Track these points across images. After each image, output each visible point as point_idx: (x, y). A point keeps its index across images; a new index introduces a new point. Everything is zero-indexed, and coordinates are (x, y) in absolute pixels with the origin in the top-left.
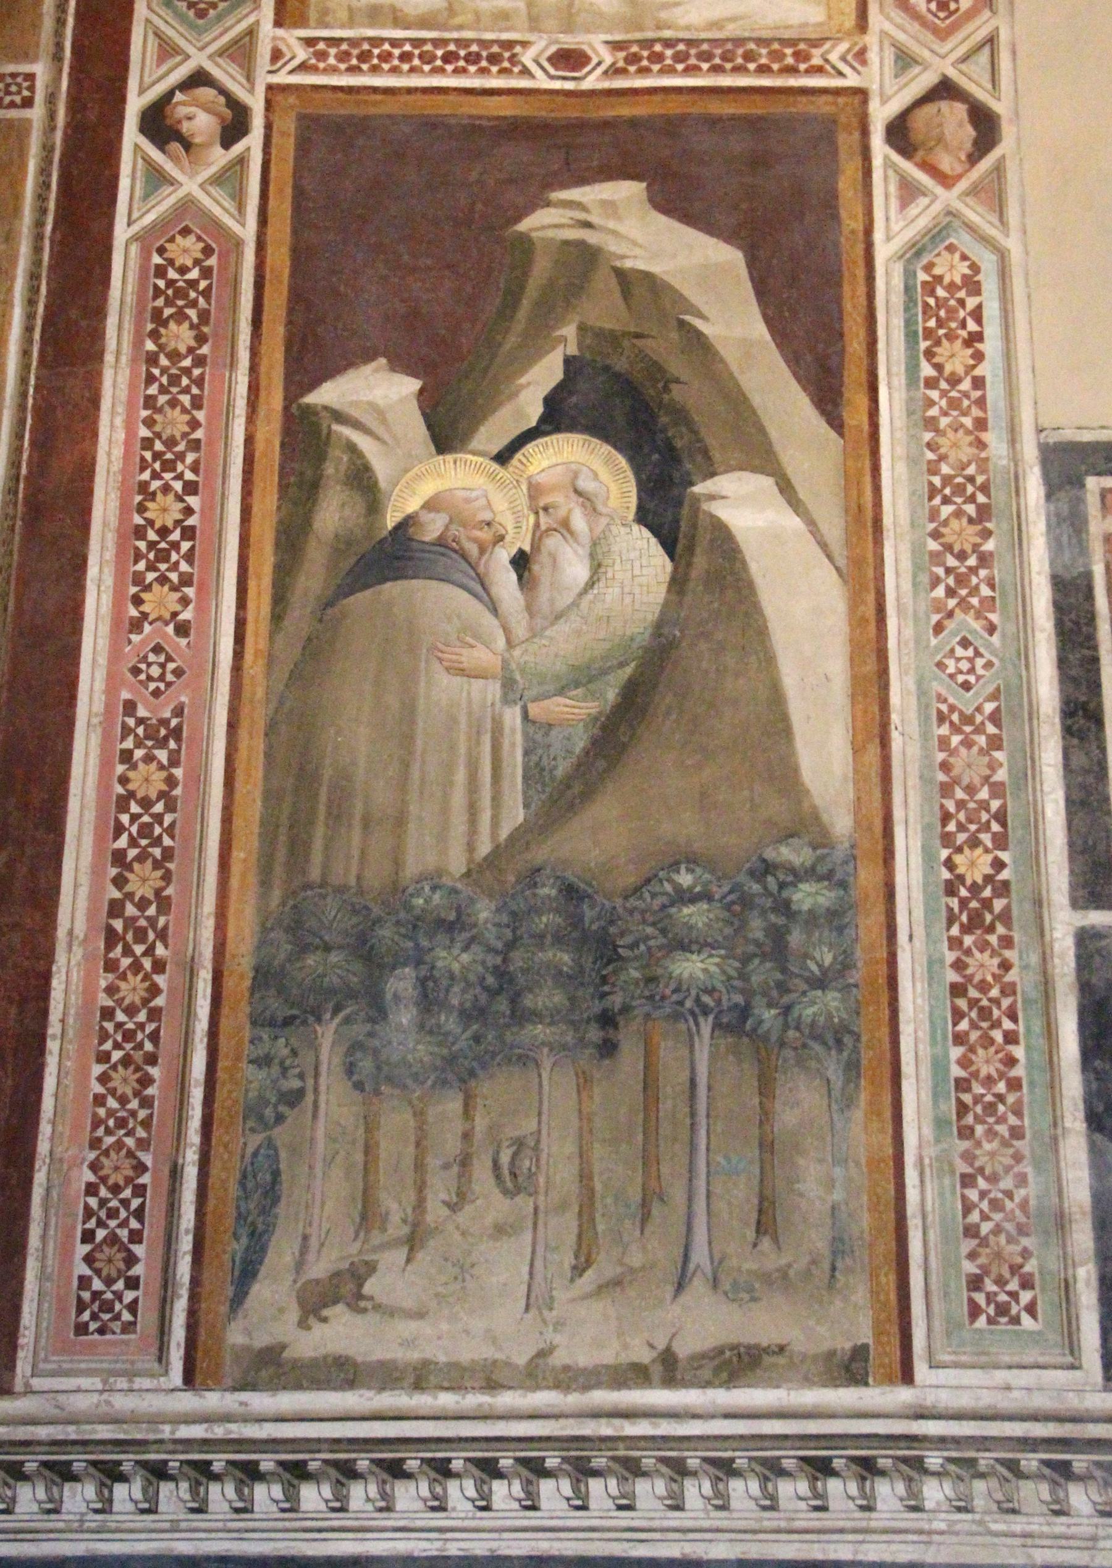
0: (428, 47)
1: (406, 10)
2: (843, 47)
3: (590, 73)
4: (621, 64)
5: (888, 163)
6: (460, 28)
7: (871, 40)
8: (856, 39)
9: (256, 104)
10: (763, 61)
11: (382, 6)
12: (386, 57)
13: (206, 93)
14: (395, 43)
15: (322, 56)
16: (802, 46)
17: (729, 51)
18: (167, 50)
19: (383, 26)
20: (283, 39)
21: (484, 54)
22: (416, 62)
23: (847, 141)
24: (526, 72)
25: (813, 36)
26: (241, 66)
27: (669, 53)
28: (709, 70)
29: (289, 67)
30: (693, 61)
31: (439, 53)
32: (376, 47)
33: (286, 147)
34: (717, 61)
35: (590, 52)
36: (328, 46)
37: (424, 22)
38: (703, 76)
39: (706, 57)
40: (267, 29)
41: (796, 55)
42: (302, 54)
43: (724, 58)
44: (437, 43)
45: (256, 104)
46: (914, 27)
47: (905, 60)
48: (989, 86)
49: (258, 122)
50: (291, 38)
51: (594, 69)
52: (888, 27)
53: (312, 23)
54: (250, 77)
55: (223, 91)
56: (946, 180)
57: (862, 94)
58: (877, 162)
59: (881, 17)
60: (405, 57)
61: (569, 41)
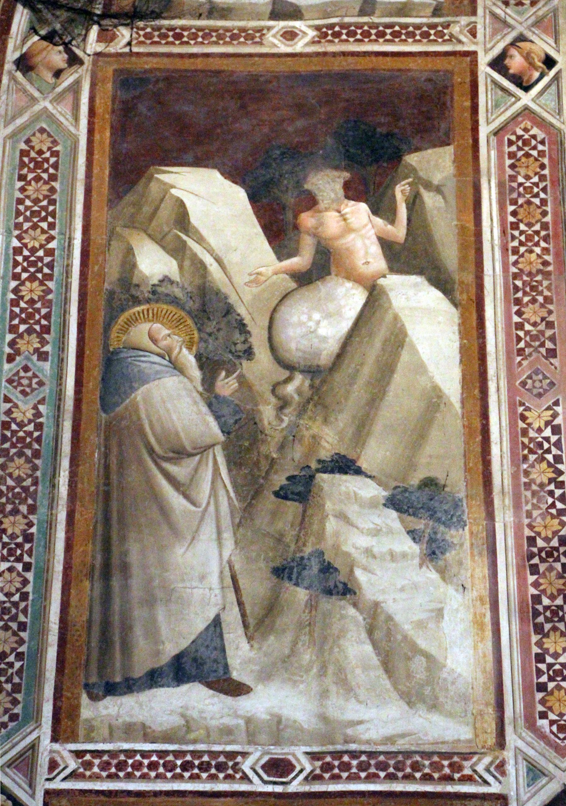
0: (170, 758)
1: (154, 727)
2: (487, 760)
3: (294, 778)
4: (318, 771)
6: (194, 742)
7: (508, 755)
8: (497, 753)
10: (427, 770)
11: (135, 724)
12: (138, 766)
14: (145, 754)
15: (88, 765)
16: (456, 759)
17: (399, 762)
19: (134, 741)
20: (58, 752)
21: (213, 763)
22: (161, 770)
24: (245, 778)
25: (464, 751)
26: (26, 776)
27: (354, 763)
28: (385, 777)
29: (62, 775)
30: (373, 770)
31: (179, 762)
32: (130, 758)
34: (391, 770)
36: (93, 757)
37: (167, 738)
38: (380, 783)
39: (383, 766)
41: (451, 765)
42: (73, 764)
43: (397, 768)
44: (178, 754)
46: (541, 745)
51: (297, 775)
52: (520, 744)
53: (81, 738)
54: (32, 785)
59: (515, 737)
60: (153, 766)
61: (278, 752)
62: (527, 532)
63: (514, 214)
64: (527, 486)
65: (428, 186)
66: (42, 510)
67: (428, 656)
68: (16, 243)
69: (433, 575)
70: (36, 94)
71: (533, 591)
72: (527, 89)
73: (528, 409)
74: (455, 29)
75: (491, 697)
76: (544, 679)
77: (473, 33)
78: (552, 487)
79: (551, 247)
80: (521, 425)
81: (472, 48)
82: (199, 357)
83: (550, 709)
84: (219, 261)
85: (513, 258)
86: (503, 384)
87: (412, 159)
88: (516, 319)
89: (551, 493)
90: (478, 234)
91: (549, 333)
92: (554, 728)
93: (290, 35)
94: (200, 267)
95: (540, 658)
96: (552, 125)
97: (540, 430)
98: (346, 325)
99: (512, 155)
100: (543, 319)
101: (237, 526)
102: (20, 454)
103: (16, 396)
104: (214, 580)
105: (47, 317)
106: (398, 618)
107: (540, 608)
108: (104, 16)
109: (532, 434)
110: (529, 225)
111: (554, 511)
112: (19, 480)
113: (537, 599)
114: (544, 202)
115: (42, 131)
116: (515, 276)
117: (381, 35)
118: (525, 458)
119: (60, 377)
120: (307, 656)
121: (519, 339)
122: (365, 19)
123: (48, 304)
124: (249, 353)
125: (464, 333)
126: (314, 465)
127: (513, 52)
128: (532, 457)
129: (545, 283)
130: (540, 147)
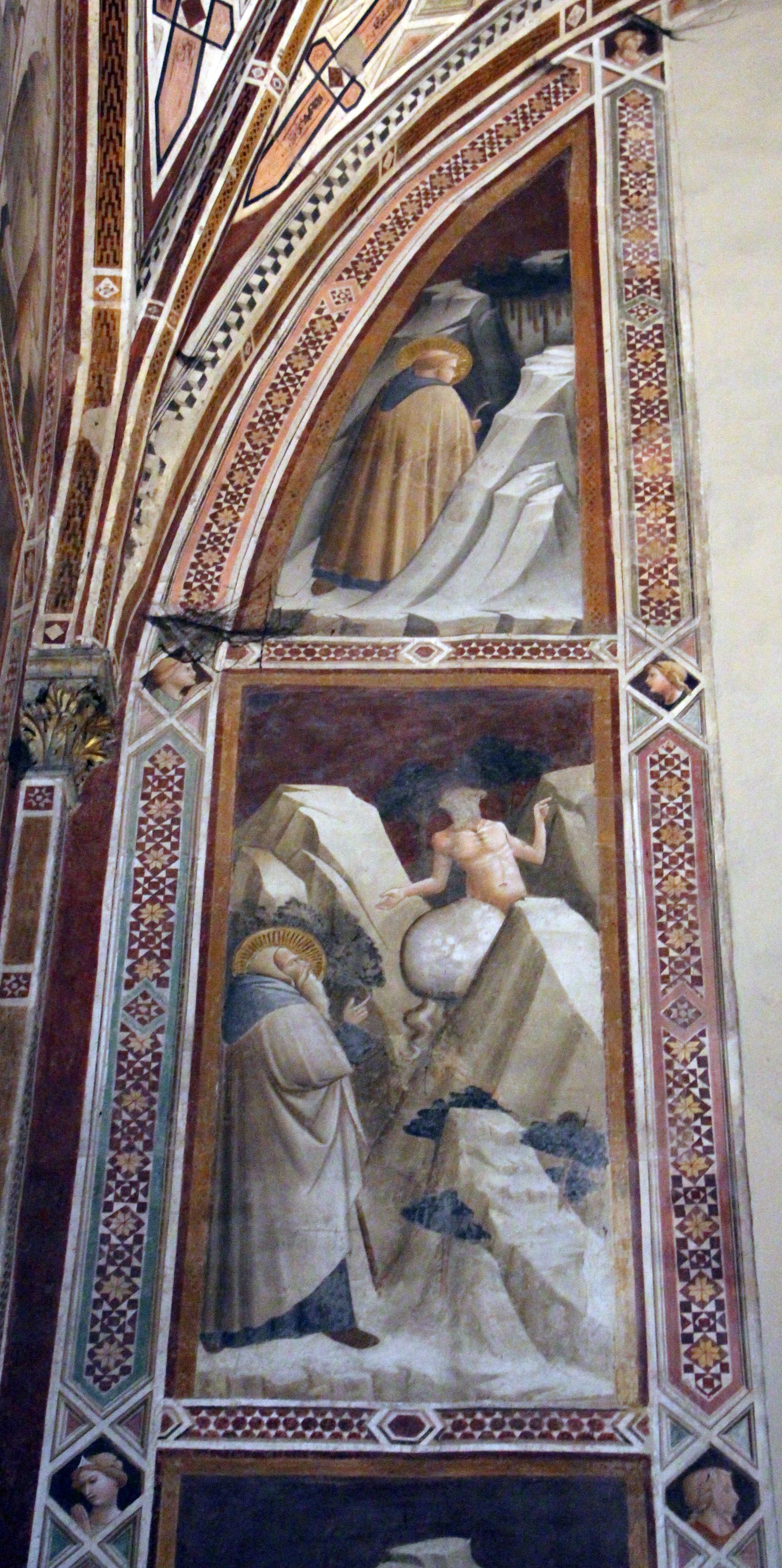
0: (291, 1415)
1: (274, 1381)
2: (629, 1417)
3: (424, 1437)
4: (449, 1430)
5: (668, 1524)
6: (317, 1397)
7: (651, 1412)
8: (640, 1410)
9: (148, 1467)
10: (565, 1429)
11: (254, 1378)
12: (256, 1424)
13: (107, 1458)
14: (265, 1411)
15: (204, 1423)
16: (596, 1416)
18: (76, 1420)
19: (254, 1396)
20: (171, 1408)
21: (337, 1421)
22: (281, 1428)
23: (634, 1502)
24: (371, 1437)
25: (604, 1407)
26: (137, 1433)
27: (488, 1420)
29: (176, 1434)
30: (507, 1428)
31: (300, 1420)
32: (249, 1415)
33: (172, 1506)
34: (527, 1428)
35: (423, 1419)
36: (210, 1414)
37: (288, 1392)
38: (516, 1442)
40: (159, 1399)
41: (591, 1424)
42: (187, 1422)
44: (299, 1411)
45: (148, 1467)
46: (686, 1401)
47: (679, 1430)
48: (748, 1455)
49: (149, 1484)
50: (179, 1406)
52: (664, 1400)
53: (196, 1393)
55: (121, 1457)
56: (716, 1541)
57: (645, 1460)
58: (660, 1522)
59: (658, 1392)
60: (273, 1424)
61: (407, 1409)
62: (673, 1171)
63: (657, 835)
64: (673, 1121)
65: (568, 805)
66: (159, 1146)
67: (567, 1305)
68: (137, 864)
69: (572, 1217)
70: (163, 711)
71: (678, 1234)
72: (669, 708)
73: (673, 1040)
74: (595, 647)
75: (634, 1351)
76: (690, 1329)
77: (614, 651)
78: (698, 1123)
79: (696, 869)
80: (666, 1056)
81: (611, 666)
82: (326, 983)
83: (696, 1362)
84: (349, 882)
85: (656, 881)
86: (647, 1011)
87: (552, 777)
88: (660, 944)
89: (697, 1130)
90: (620, 856)
91: (694, 959)
92: (700, 1383)
93: (425, 652)
94: (329, 888)
95: (686, 1307)
96: (695, 745)
97: (685, 1063)
98: (481, 951)
99: (654, 775)
100: (688, 945)
101: (365, 1164)
102: (137, 1087)
103: (133, 1024)
104: (340, 1222)
105: (168, 940)
106: (536, 1264)
107: (685, 1253)
108: (233, 633)
109: (677, 1066)
110: (674, 847)
111: (700, 1149)
112: (135, 1114)
113: (682, 1243)
114: (688, 823)
115: (167, 748)
116: (659, 900)
117: (519, 652)
118: (670, 1092)
119: (180, 1004)
120: (438, 1304)
121: (663, 966)
122: (503, 636)
123: (169, 927)
124: (379, 979)
125: (605, 958)
126: (447, 1098)
127: (654, 670)
128: (678, 1091)
129: (690, 907)
130: (684, 767)
